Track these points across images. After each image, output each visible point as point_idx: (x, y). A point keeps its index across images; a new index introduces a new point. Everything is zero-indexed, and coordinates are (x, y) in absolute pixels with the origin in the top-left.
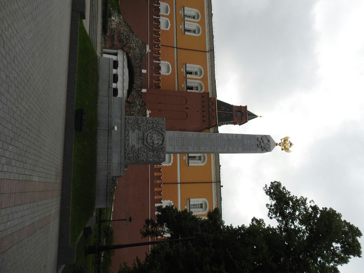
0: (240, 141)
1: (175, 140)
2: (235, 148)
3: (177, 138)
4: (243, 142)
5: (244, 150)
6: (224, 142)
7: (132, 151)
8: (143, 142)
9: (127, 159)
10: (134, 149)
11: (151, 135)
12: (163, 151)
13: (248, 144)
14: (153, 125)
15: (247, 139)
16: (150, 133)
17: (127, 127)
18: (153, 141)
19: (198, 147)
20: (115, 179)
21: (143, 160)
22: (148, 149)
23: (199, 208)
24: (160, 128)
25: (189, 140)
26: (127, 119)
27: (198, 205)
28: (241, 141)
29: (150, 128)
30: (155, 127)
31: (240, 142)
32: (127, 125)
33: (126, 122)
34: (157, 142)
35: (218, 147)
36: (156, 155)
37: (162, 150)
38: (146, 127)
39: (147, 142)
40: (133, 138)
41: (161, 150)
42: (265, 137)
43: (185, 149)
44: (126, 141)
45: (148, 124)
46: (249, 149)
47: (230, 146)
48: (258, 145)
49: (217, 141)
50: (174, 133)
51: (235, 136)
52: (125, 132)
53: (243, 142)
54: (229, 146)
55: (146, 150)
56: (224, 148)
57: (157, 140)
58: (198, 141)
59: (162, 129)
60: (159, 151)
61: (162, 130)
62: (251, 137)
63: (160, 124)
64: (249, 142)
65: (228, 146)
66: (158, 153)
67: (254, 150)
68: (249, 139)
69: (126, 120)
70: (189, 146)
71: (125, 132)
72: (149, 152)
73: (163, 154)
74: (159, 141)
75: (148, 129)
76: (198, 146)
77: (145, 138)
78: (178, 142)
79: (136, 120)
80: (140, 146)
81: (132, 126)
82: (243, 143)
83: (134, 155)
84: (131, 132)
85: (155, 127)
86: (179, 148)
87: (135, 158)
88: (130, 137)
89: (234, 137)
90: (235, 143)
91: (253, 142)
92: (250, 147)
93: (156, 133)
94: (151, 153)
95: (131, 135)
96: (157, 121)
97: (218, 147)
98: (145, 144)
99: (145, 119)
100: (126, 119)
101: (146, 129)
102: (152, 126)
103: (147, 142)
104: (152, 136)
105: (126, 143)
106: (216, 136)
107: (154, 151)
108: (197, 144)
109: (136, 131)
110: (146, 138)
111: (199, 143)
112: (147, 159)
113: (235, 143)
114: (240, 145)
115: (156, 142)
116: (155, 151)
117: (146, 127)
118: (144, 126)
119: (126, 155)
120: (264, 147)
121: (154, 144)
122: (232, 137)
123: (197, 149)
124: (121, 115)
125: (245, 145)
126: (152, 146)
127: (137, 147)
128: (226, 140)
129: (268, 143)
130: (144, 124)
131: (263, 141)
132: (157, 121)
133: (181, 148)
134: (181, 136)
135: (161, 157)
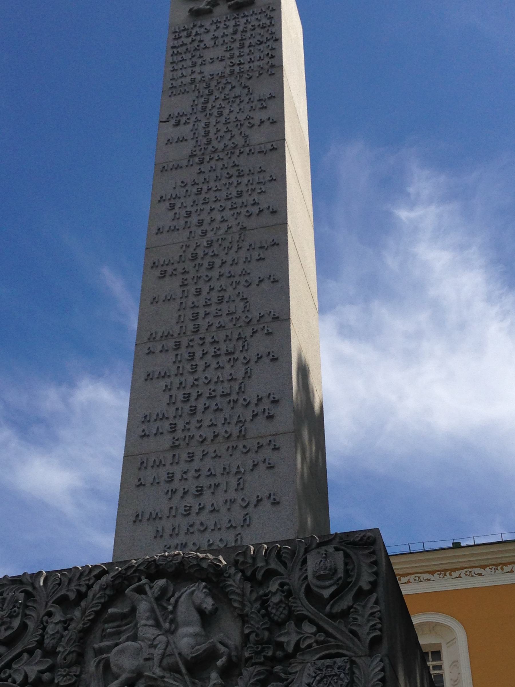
0: (212, 98)
1: (190, 500)
2: (258, 116)
3: (174, 492)
4: (214, 83)
5: (273, 66)
6: (218, 179)
13: (228, 55)
15: (194, 65)
18: (174, 669)
24: (58, 617)
25: (199, 396)
28: (211, 93)
30: (49, 662)
31: (216, 94)
34: (195, 629)
35: (255, 210)
36: (320, 629)
41: (274, 586)
43: (270, 417)
46: (261, 47)
47: (239, 140)
49: (207, 220)
51: (177, 124)
53: (214, 83)
54: (247, 149)
56: (261, 171)
57: (167, 625)
58: (209, 340)
59: (72, 596)
61: (81, 596)
63: (16, 623)
64: (219, 52)
65: (241, 153)
67: (271, 18)
68: (198, 53)
73: (305, 562)
74: (182, 608)
76: (248, 331)
78: (211, 475)
82: (224, 81)
85: (49, 662)
86: (262, 467)
89: (185, 130)
90: (222, 119)
92: (247, 43)
93: (100, 651)
97: (255, 210)
106: (173, 230)
107: (280, 645)
108: (228, 339)
111: (221, 327)
113: (222, 119)
114: (238, 91)
116: (283, 639)
123: (269, 334)
125: (237, 69)
128: (201, 172)
133: (267, 452)
134: (160, 464)
135: (341, 573)
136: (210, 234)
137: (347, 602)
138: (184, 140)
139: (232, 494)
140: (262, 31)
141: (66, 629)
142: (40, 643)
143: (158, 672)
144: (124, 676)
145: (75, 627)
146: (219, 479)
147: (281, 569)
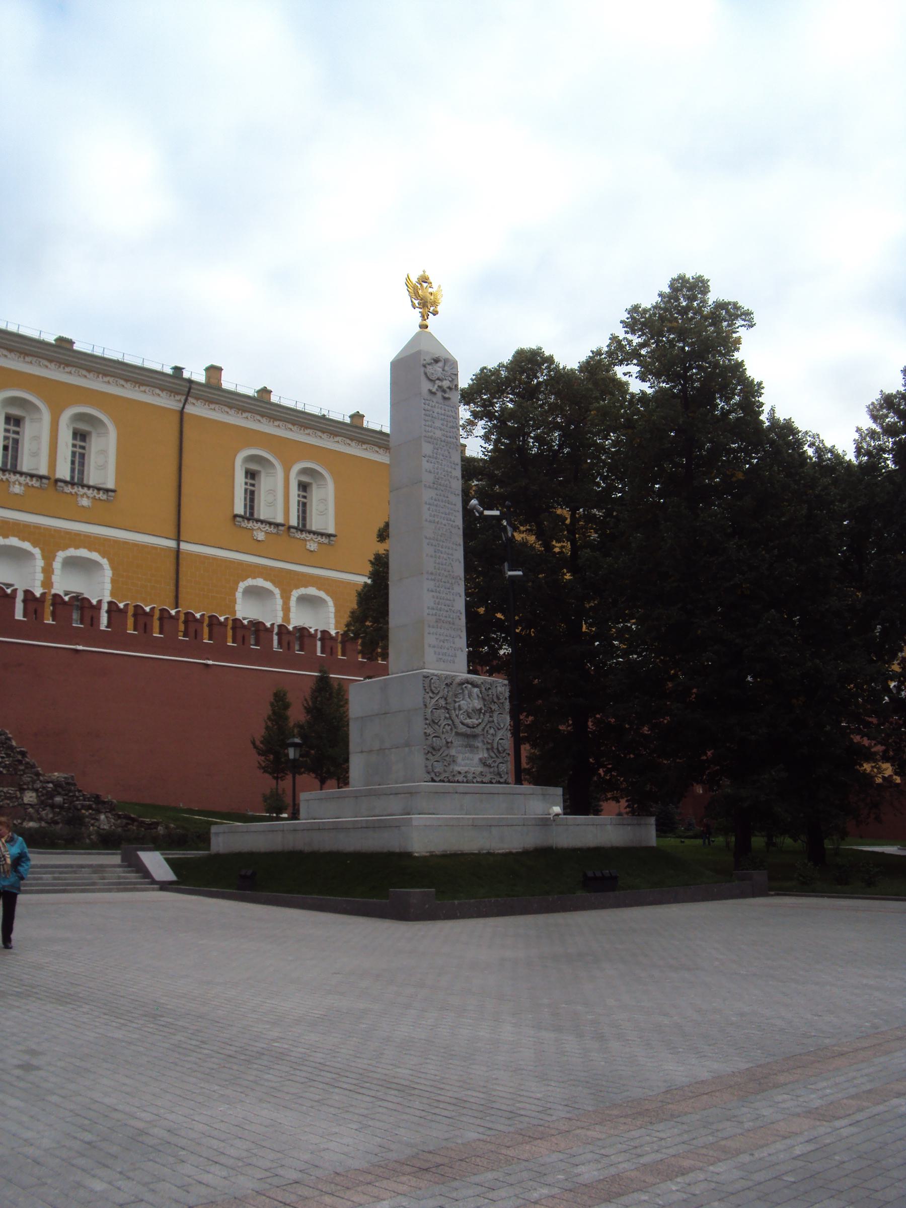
1: (442, 643)
8: (475, 736)
10: (490, 761)
11: (461, 714)
16: (457, 716)
19: (455, 583)
20: (51, 785)
23: (17, 433)
24: (446, 690)
26: (433, 775)
27: (7, 434)
29: (447, 715)
33: (439, 779)
37: (489, 688)
38: (446, 726)
39: (478, 725)
40: (467, 761)
42: (428, 366)
45: (440, 720)
48: (445, 398)
50: (430, 646)
52: (458, 782)
55: (492, 731)
58: (443, 580)
60: (491, 696)
62: (427, 412)
63: (439, 689)
66: (495, 700)
69: (435, 778)
70: (453, 606)
73: (496, 687)
77: (469, 731)
80: (480, 745)
81: (446, 763)
84: (458, 768)
87: (505, 759)
88: (466, 769)
91: (440, 411)
95: (462, 768)
99: (430, 727)
100: (432, 778)
102: (443, 711)
103: (478, 725)
104: (464, 712)
105: (479, 780)
106: (430, 522)
109: (453, 752)
110: (469, 727)
112: (507, 729)
113: (443, 467)
114: (446, 453)
115: (478, 704)
117: (447, 726)
119: (502, 780)
120: (450, 381)
121: (481, 709)
122: (430, 472)
124: (457, 793)
126: (484, 714)
127: (483, 754)
129: (440, 364)
131: (438, 379)
132: (431, 694)
134: (433, 627)
136: (441, 529)
138: (431, 472)
139: (452, 645)
140: (454, 420)
143: (471, 711)
144: (464, 710)
145: (451, 693)
146: (447, 638)
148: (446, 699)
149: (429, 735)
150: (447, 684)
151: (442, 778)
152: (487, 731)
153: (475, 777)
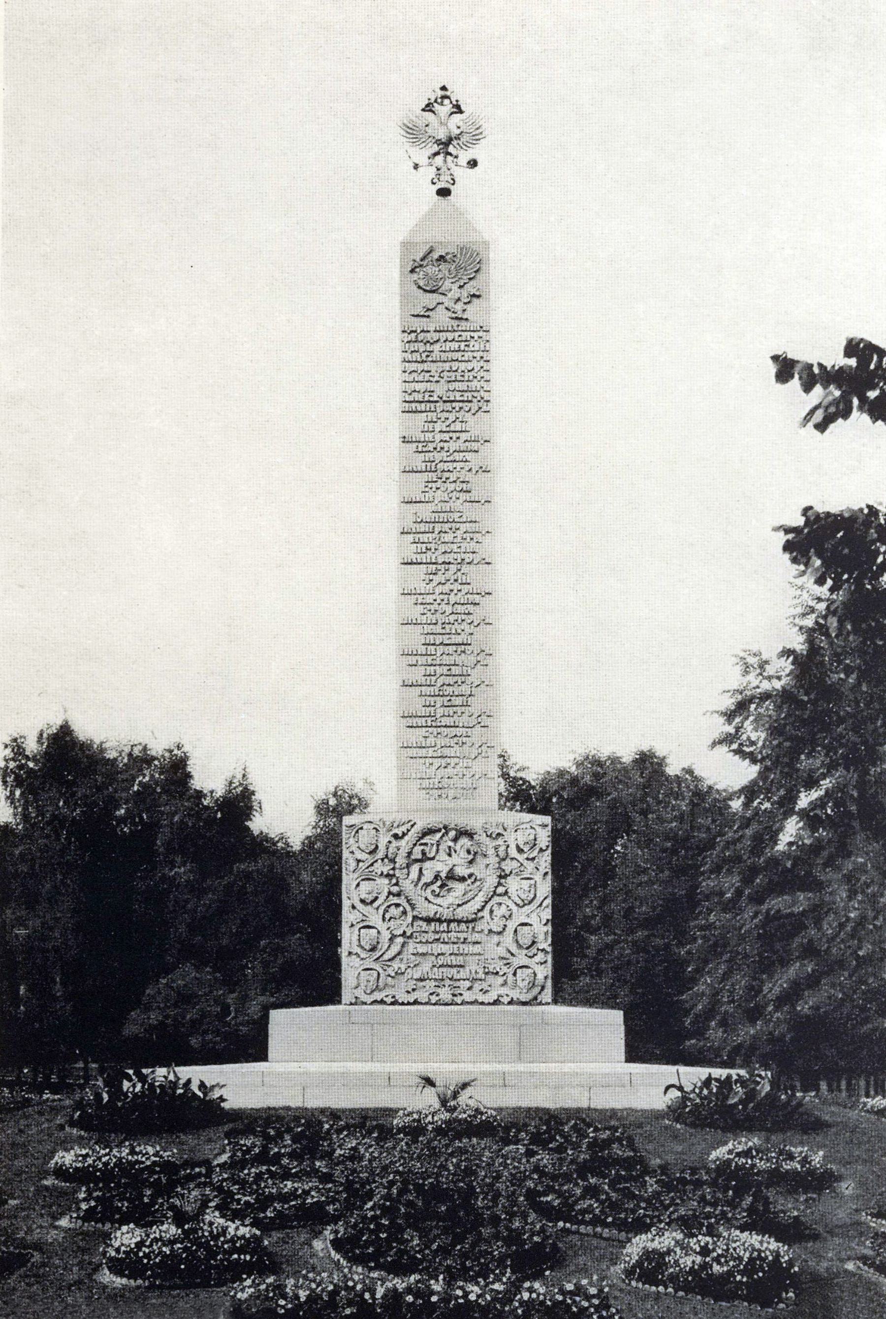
7: (505, 969)
9: (540, 993)
12: (501, 831)
14: (382, 873)
17: (393, 997)
21: (544, 922)
22: (497, 899)
26: (359, 993)
32: (387, 996)
37: (499, 835)
41: (500, 841)
44: (459, 1000)
61: (404, 834)
71: (421, 1004)
72: (509, 897)
75: (402, 901)
79: (363, 955)
83: (525, 961)
94: (513, 885)
96: (360, 855)
98: (474, 916)
101: (401, 909)
107: (504, 871)
112: (541, 905)
118: (387, 916)
130: (375, 919)
137: (535, 853)
141: (398, 850)
142: (387, 856)
147: (504, 833)
148: (393, 861)
149: (352, 925)
150: (396, 836)
151: (378, 996)
152: (491, 912)
153: (461, 995)
